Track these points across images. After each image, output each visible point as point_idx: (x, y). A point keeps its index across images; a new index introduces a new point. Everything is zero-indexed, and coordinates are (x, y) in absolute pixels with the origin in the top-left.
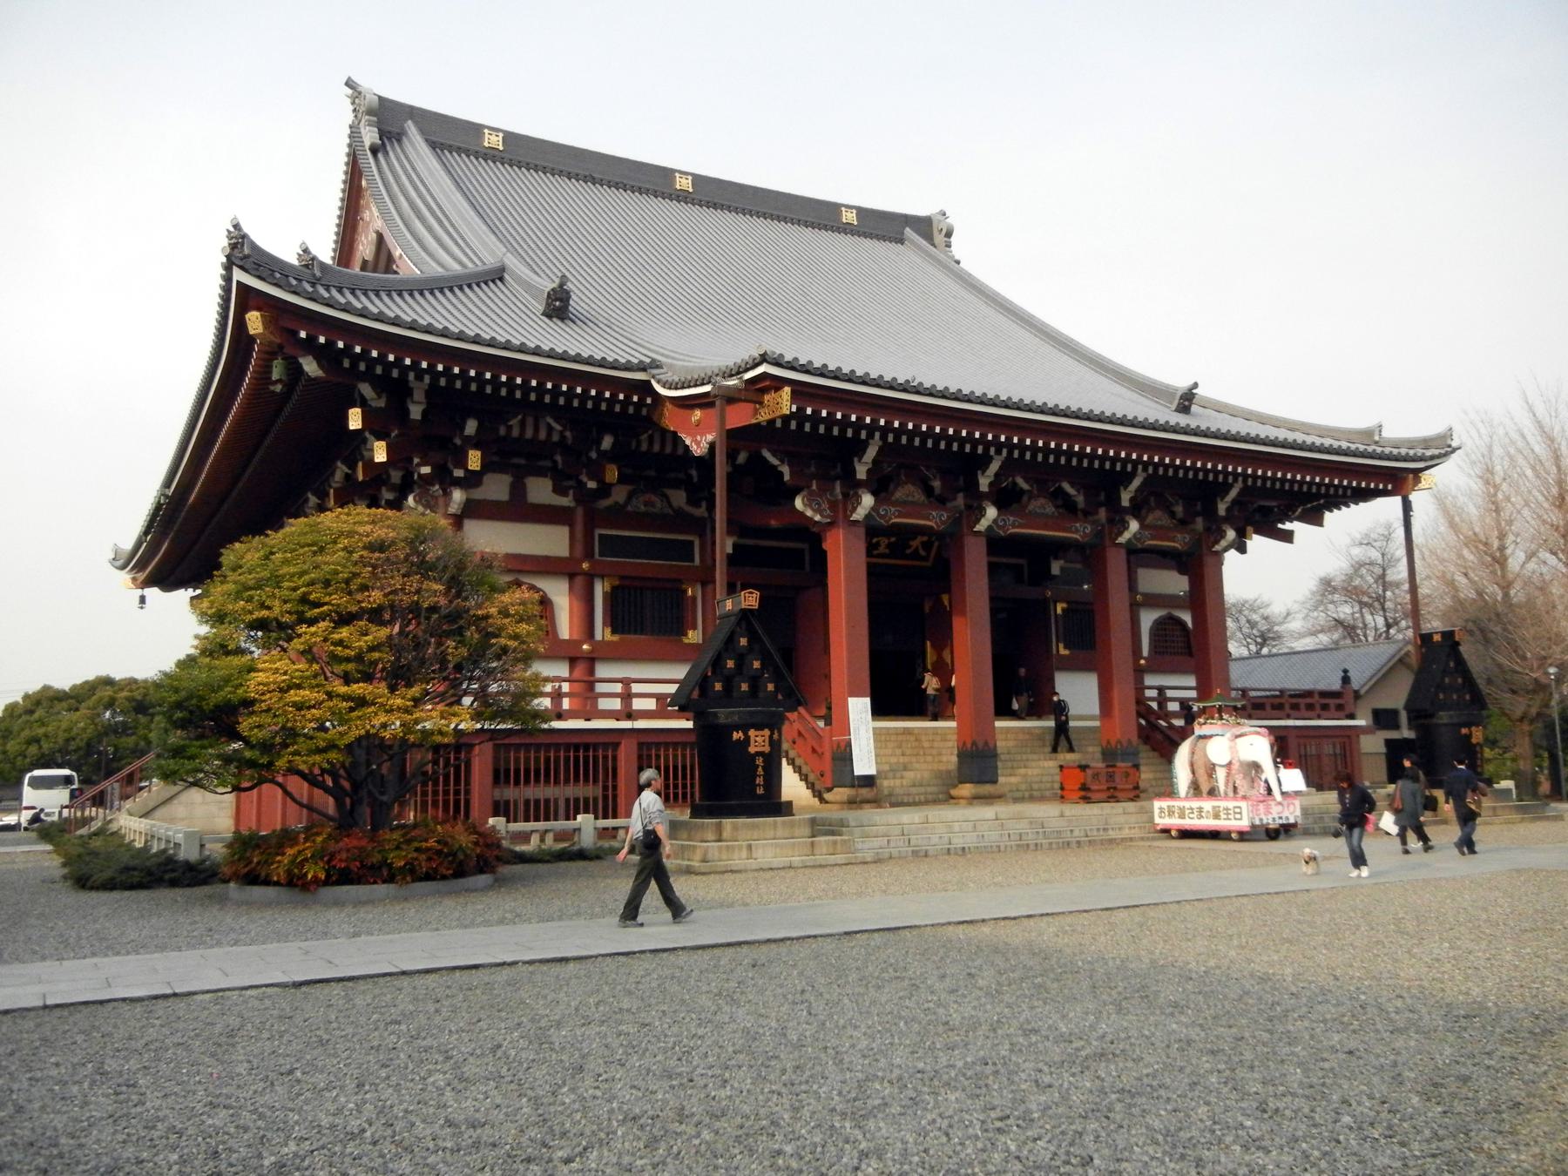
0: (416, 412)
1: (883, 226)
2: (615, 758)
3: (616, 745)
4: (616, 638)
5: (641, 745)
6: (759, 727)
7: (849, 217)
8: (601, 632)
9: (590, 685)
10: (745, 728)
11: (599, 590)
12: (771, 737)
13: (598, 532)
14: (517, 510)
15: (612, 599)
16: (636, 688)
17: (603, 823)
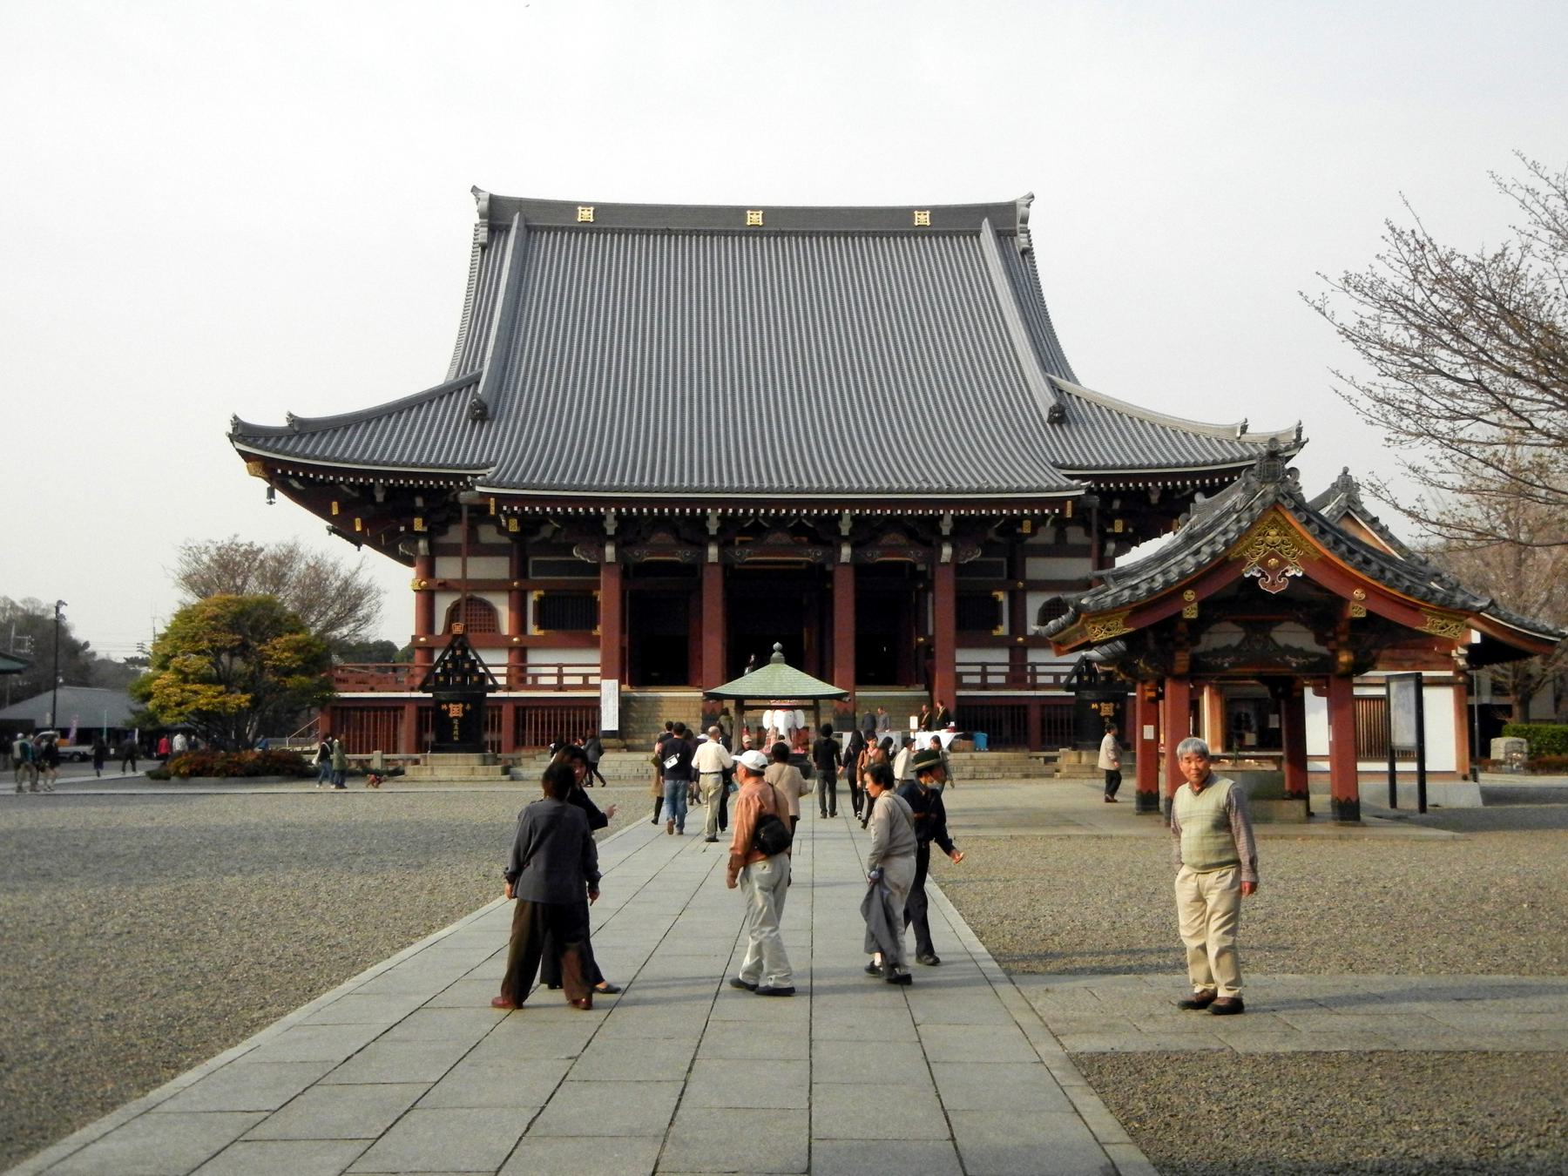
0: (380, 497)
1: (956, 223)
2: (500, 717)
3: (500, 708)
4: (541, 633)
5: (517, 709)
6: (456, 702)
7: (923, 219)
8: (533, 630)
9: (523, 669)
10: (448, 703)
11: (533, 598)
12: (464, 710)
13: (531, 560)
14: (476, 548)
15: (540, 605)
16: (566, 670)
17: (386, 756)
